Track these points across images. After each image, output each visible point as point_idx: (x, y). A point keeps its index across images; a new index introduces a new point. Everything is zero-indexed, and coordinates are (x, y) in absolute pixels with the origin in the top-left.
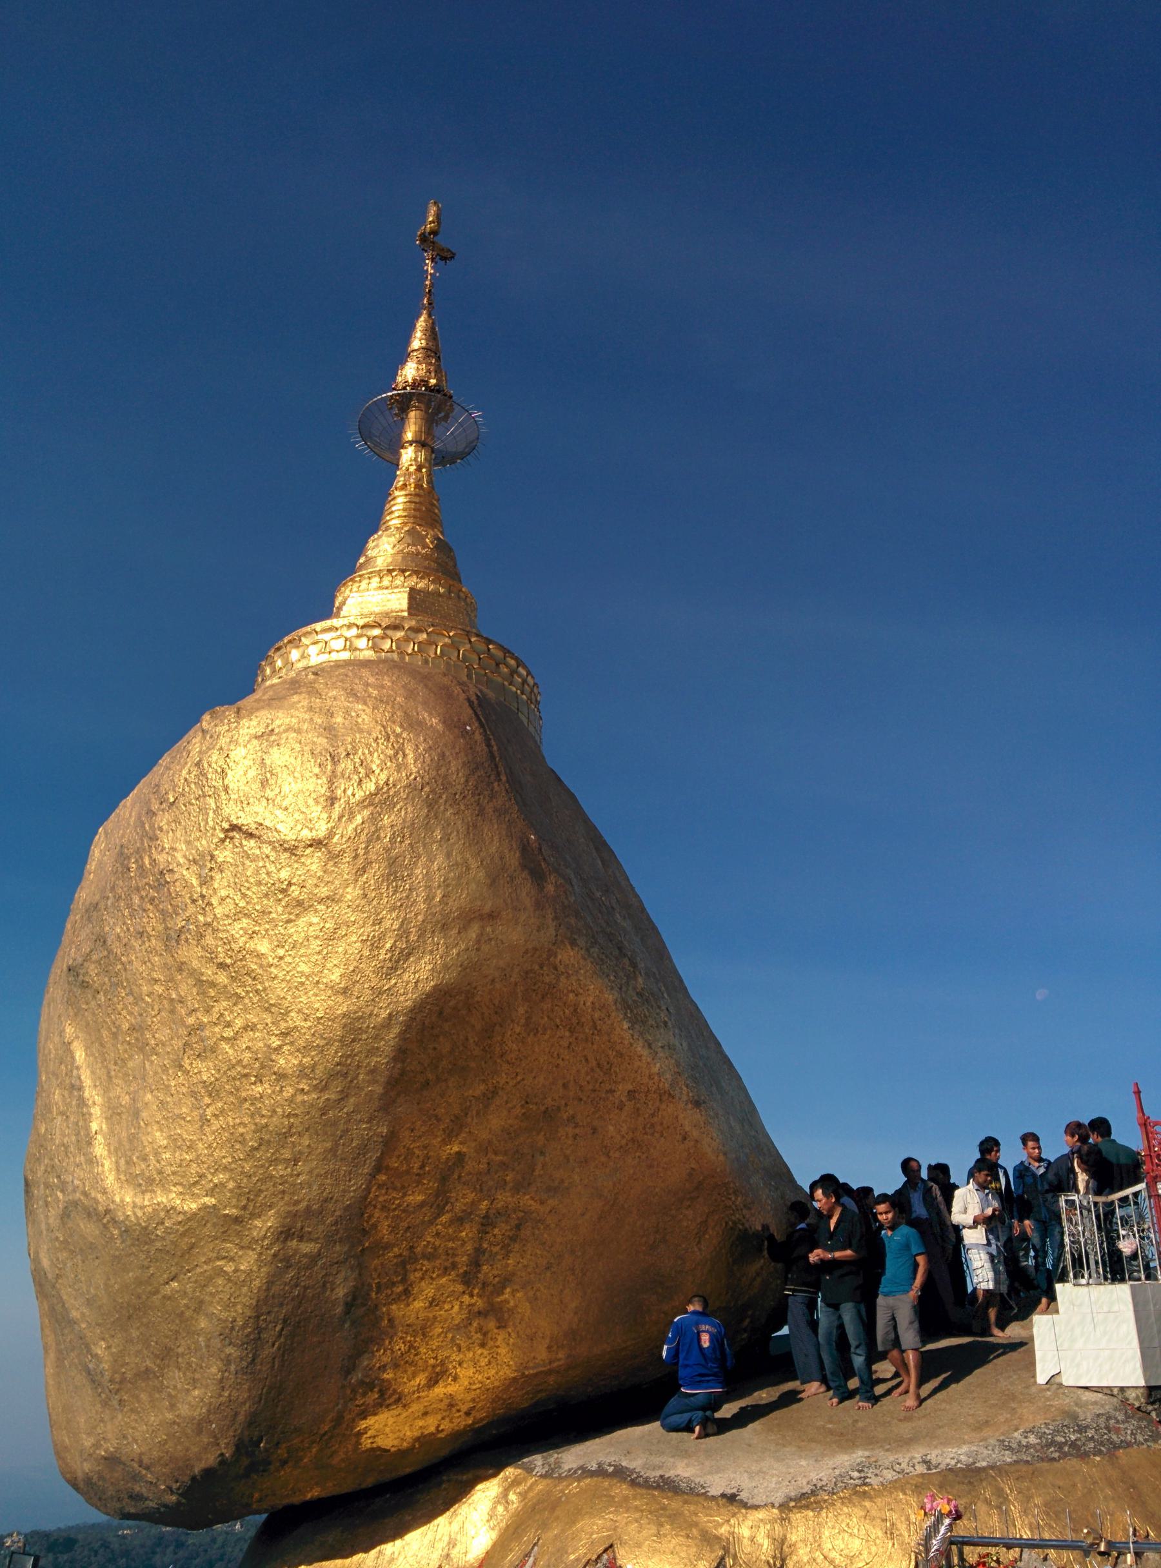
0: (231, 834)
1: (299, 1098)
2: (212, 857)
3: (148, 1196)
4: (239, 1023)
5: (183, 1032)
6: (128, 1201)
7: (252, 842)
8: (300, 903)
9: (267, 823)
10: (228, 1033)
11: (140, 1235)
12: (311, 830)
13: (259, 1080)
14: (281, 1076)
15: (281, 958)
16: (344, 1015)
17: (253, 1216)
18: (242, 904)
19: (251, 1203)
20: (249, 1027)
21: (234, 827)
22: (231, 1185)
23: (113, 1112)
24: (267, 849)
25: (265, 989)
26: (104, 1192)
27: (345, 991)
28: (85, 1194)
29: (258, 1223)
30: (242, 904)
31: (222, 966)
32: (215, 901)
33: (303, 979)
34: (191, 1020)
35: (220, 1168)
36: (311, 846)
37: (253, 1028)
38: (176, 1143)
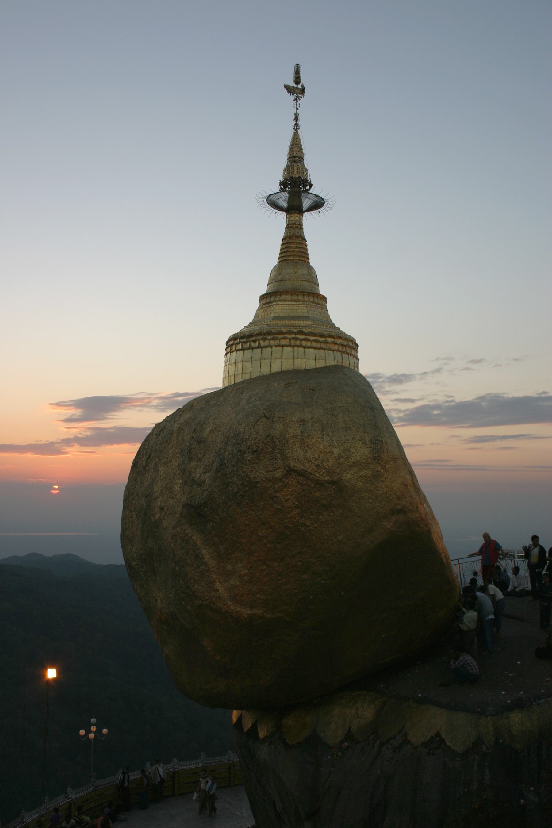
1: (323, 582)
9: (308, 470)
12: (330, 476)
15: (316, 528)
30: (297, 503)
33: (326, 537)
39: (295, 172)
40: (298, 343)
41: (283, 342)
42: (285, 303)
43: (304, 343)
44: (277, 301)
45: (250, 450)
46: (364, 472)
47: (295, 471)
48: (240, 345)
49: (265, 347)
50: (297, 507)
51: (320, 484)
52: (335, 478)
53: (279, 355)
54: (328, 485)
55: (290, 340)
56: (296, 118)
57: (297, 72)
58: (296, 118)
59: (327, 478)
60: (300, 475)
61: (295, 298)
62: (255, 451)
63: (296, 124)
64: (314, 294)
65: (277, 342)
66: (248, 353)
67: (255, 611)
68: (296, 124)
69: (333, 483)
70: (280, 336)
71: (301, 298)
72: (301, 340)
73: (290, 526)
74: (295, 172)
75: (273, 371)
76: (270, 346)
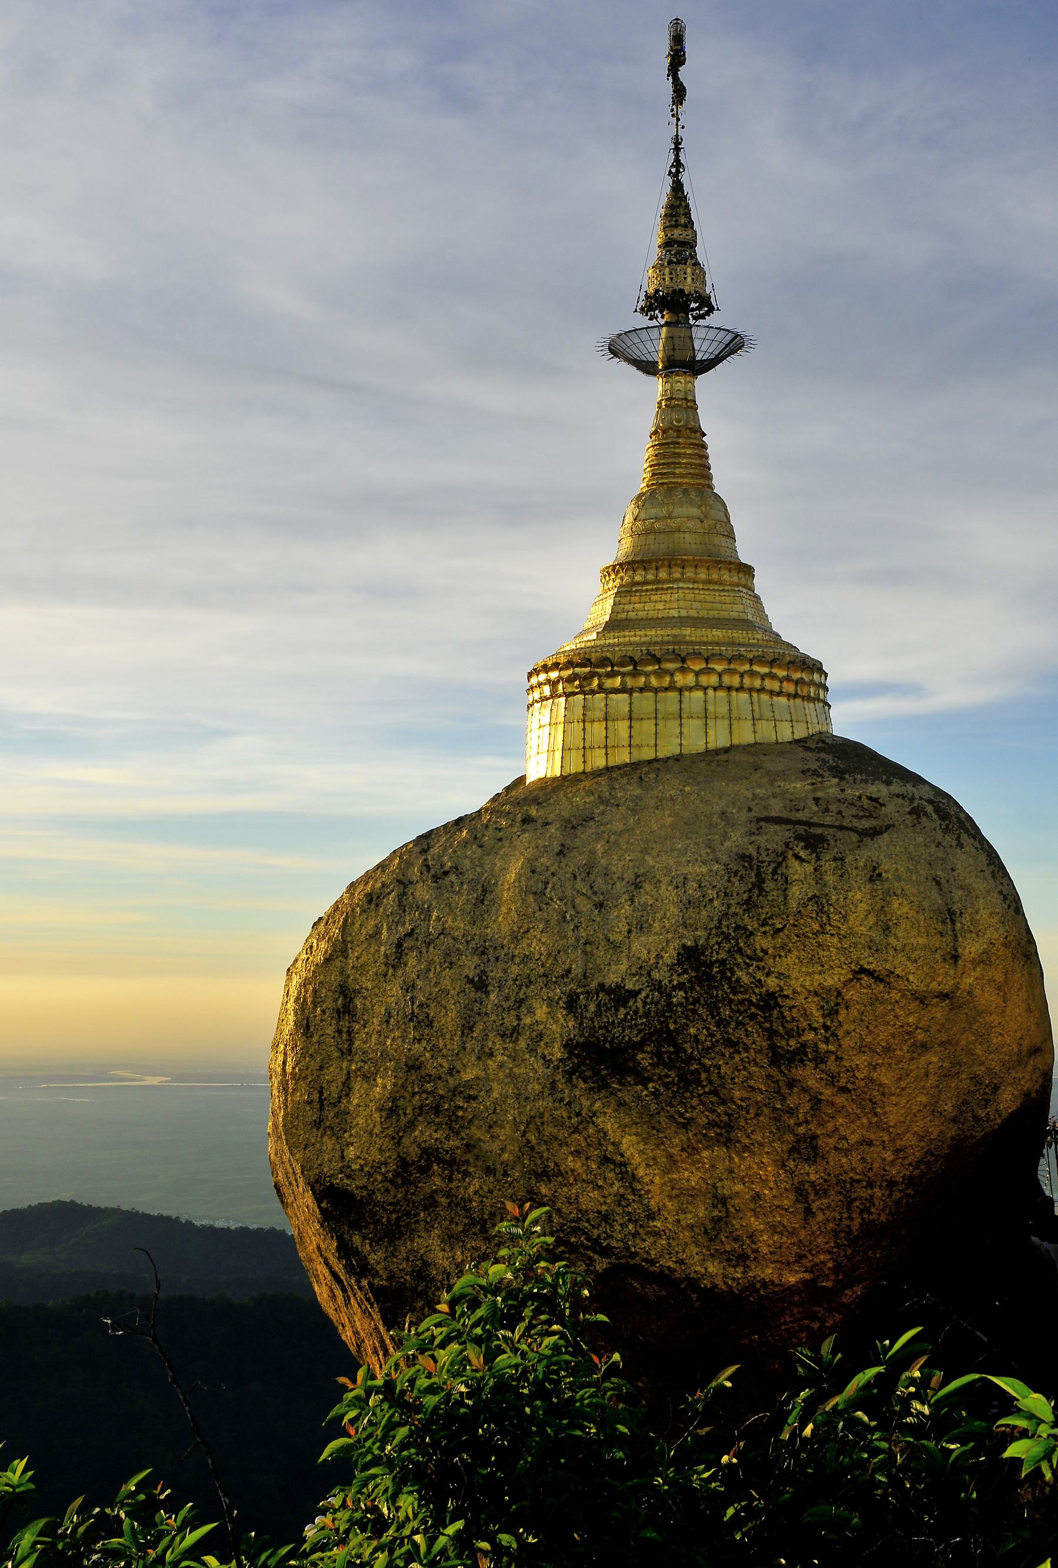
0: (859, 976)
3: (740, 1269)
4: (853, 1139)
5: (789, 1137)
15: (903, 1089)
16: (952, 1138)
21: (863, 970)
22: (830, 1265)
25: (885, 1113)
27: (954, 1120)
29: (848, 1292)
31: (844, 1090)
32: (840, 1033)
34: (802, 1130)
36: (937, 997)
37: (870, 1143)
38: (774, 1229)
39: (689, 280)
40: (757, 683)
42: (696, 586)
43: (769, 684)
44: (678, 580)
45: (767, 928)
47: (870, 973)
48: (619, 679)
49: (690, 689)
53: (723, 709)
54: (935, 1001)
55: (742, 676)
56: (677, 149)
57: (678, 38)
58: (677, 149)
59: (934, 985)
62: (778, 931)
63: (678, 164)
64: (731, 563)
65: (714, 680)
66: (645, 702)
68: (678, 164)
72: (763, 677)
74: (689, 280)
75: (711, 746)
76: (698, 686)
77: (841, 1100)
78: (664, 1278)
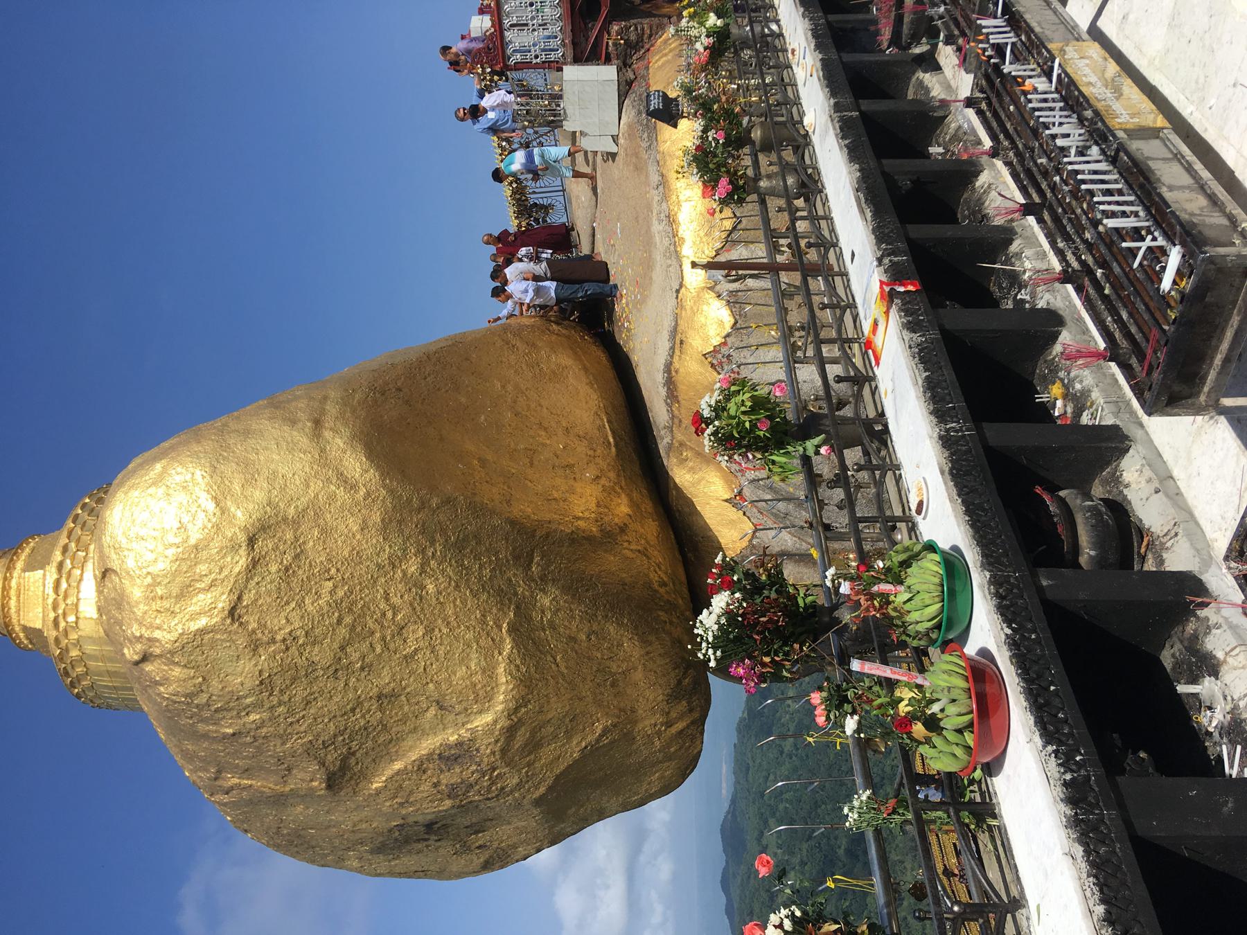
2: (254, 631)
6: (500, 701)
7: (245, 597)
8: (297, 556)
10: (389, 615)
11: (527, 685)
13: (423, 587)
14: (422, 571)
15: (338, 570)
17: (516, 594)
18: (293, 605)
19: (504, 596)
20: (387, 598)
21: (232, 612)
23: (440, 724)
24: (253, 583)
25: (360, 584)
26: (495, 722)
28: (497, 741)
35: (484, 622)
38: (464, 660)
41: (71, 619)
46: (237, 487)
50: (300, 605)
51: (255, 563)
52: (242, 538)
59: (243, 551)
60: (240, 598)
61: (13, 593)
67: (501, 670)
69: (251, 541)
70: (62, 625)
71: (14, 583)
73: (336, 614)
77: (348, 620)
78: (511, 732)
